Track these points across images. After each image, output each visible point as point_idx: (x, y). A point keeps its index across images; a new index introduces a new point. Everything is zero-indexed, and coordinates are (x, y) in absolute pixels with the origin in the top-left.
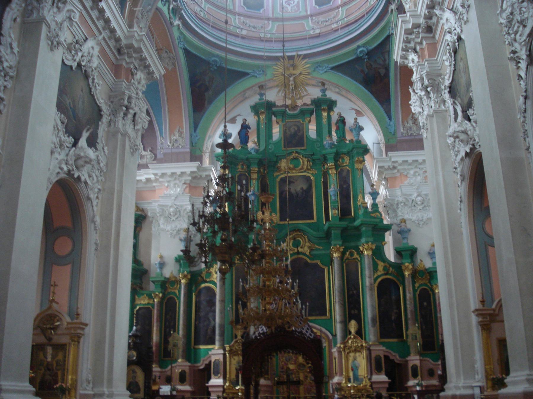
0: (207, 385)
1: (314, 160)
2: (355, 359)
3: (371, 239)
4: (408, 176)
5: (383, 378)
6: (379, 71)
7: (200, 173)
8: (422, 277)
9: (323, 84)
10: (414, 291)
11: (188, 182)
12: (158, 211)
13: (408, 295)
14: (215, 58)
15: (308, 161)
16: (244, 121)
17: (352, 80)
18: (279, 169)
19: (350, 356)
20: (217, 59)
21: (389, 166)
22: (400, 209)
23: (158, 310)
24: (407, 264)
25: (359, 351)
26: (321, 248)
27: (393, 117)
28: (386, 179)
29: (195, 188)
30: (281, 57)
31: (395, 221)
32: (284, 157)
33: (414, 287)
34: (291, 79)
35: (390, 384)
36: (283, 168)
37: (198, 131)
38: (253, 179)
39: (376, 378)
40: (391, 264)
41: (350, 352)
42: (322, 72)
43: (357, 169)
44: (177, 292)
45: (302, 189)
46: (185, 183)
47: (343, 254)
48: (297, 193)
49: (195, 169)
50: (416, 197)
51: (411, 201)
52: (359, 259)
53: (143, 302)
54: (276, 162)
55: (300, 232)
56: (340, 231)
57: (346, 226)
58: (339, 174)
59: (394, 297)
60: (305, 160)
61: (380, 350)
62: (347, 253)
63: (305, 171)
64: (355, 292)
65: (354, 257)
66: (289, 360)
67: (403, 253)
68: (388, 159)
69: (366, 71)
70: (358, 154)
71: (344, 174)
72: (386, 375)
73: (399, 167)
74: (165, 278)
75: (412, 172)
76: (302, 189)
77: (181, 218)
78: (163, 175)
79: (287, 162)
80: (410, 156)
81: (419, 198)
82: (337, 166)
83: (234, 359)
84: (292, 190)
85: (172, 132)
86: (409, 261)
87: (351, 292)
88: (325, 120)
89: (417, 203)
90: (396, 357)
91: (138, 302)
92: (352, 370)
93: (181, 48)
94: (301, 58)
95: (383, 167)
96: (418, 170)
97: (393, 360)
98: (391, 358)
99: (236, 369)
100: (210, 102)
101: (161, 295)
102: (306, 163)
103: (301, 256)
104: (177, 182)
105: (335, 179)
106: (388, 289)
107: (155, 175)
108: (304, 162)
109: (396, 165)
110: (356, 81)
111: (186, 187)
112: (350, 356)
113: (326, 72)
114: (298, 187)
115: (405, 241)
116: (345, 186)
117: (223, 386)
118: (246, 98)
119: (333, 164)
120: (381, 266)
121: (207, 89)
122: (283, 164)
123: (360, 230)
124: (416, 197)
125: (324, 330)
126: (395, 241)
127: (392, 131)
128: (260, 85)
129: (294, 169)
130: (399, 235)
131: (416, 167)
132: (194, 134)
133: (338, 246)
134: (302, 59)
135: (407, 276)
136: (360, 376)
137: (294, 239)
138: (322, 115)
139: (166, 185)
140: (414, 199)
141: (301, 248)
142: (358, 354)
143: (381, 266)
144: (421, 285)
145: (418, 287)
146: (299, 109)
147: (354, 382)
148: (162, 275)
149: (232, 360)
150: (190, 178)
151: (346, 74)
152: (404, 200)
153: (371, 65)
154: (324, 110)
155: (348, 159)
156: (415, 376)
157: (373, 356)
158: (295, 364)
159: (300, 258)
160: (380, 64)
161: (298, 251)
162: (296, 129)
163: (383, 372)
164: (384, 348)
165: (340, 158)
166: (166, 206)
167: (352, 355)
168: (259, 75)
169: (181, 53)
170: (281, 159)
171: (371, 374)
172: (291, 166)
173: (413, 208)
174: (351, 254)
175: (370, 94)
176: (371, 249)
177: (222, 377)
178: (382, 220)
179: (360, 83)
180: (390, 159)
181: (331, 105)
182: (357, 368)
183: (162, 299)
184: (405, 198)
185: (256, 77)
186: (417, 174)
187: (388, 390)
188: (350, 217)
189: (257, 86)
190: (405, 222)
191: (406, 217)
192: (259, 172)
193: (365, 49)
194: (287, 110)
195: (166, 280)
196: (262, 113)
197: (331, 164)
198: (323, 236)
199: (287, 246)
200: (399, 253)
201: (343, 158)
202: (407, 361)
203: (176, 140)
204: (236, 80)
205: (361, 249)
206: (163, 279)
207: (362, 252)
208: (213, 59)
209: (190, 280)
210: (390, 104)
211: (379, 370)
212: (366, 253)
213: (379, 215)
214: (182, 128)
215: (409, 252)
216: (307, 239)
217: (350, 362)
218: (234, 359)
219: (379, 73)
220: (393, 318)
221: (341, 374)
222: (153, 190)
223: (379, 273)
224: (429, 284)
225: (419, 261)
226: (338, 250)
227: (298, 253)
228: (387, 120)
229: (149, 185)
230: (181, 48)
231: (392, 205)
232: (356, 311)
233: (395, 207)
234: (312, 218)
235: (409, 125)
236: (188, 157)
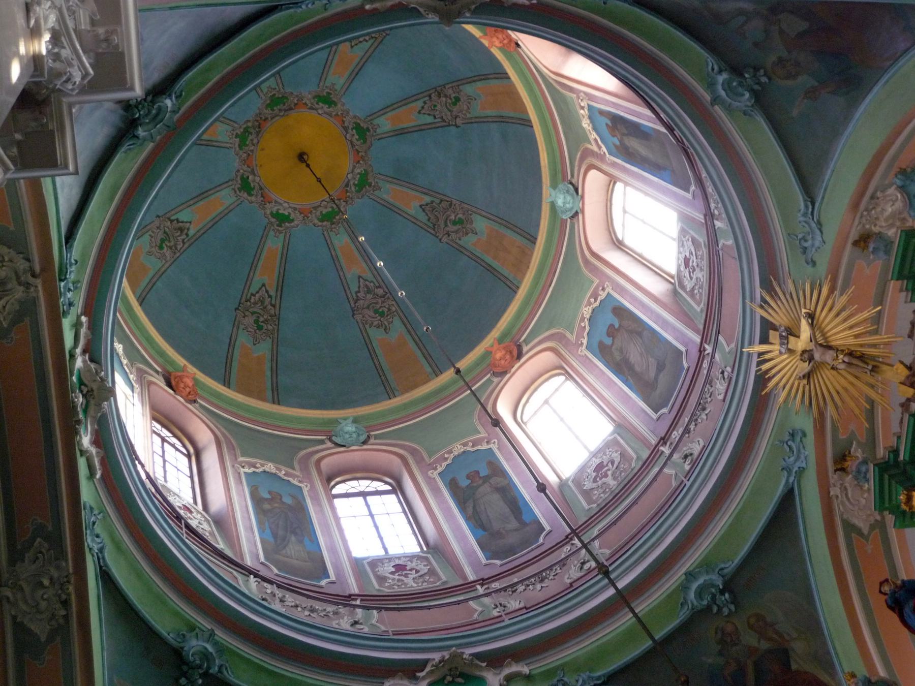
17: (847, 133)
20: (701, 581)
30: (760, 363)
42: (819, 238)
69: (805, 81)
94: (768, 299)
113: (819, 224)
121: (783, 655)
134: (772, 297)
153: (780, 60)
179: (853, 105)
189: (833, 478)
193: (721, 78)
204: (795, 539)
208: (692, 595)
219: (801, 35)
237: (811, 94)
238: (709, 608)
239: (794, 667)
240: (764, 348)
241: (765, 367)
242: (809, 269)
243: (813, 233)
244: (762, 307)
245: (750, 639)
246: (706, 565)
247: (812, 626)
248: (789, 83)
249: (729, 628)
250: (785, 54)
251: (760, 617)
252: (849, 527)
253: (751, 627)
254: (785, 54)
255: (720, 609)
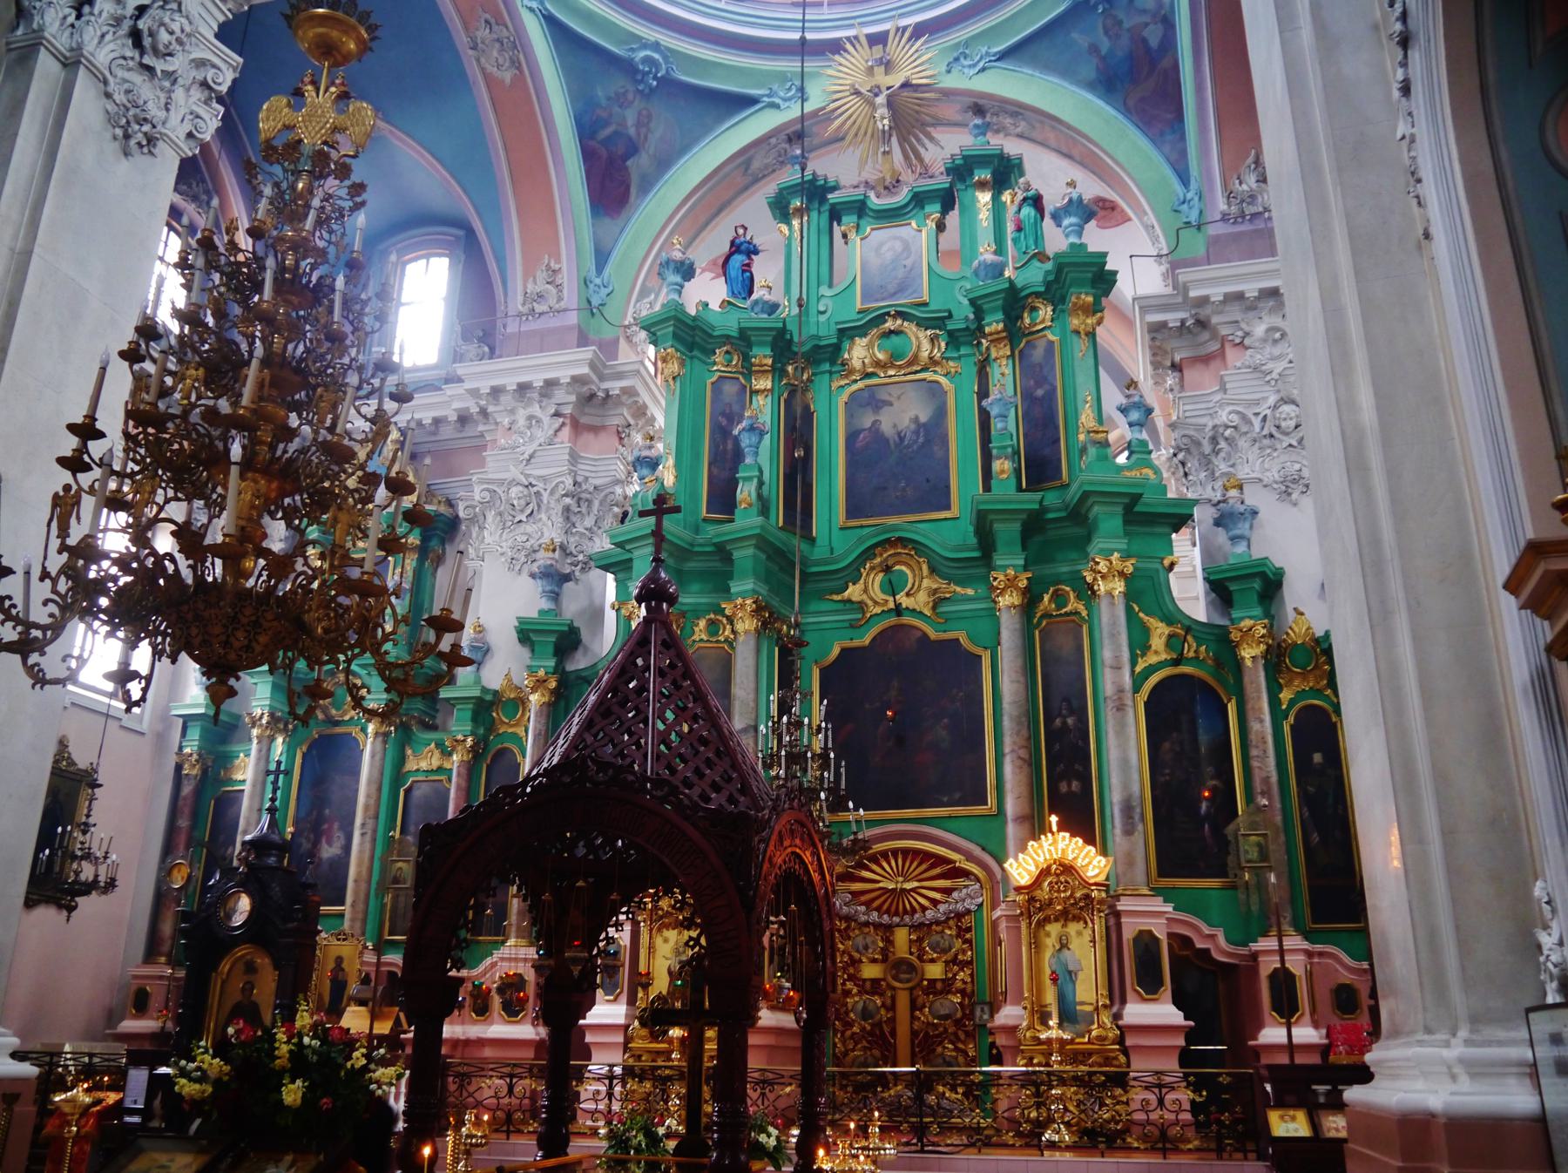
0: (581, 1022)
1: (951, 334)
2: (1064, 945)
3: (1122, 544)
4: (1247, 342)
5: (1165, 1012)
6: (1146, 33)
7: (606, 385)
8: (1303, 668)
9: (979, 110)
10: (1277, 715)
11: (567, 410)
12: (477, 498)
13: (1259, 732)
14: (648, 53)
15: (933, 340)
16: (741, 231)
17: (1066, 84)
18: (846, 370)
19: (1048, 935)
20: (656, 56)
21: (1183, 322)
22: (1222, 454)
23: (458, 787)
24: (1247, 623)
25: (1077, 918)
26: (970, 592)
27: (1194, 171)
28: (1176, 367)
29: (595, 429)
30: (848, 39)
31: (1208, 493)
32: (862, 331)
33: (1274, 702)
34: (881, 100)
35: (1191, 1036)
36: (857, 364)
37: (608, 270)
38: (757, 392)
39: (1137, 1012)
40: (1190, 627)
41: (1047, 920)
42: (972, 72)
43: (1078, 332)
44: (520, 731)
45: (916, 420)
46: (557, 414)
47: (1030, 599)
48: (899, 434)
49: (585, 370)
50: (1275, 407)
51: (1257, 422)
52: (1084, 613)
53: (424, 765)
54: (836, 349)
55: (905, 547)
56: (1017, 526)
57: (1036, 506)
58: (1020, 358)
59: (1204, 738)
60: (924, 336)
61: (1150, 914)
62: (1046, 598)
63: (924, 369)
64: (1070, 721)
65: (1068, 609)
66: (866, 948)
67: (1233, 587)
68: (1180, 300)
69: (1105, 45)
70: (1079, 283)
71: (1038, 354)
72: (1175, 1003)
73: (1215, 320)
74: (484, 690)
75: (1259, 330)
76: (916, 420)
77: (543, 516)
78: (496, 392)
79: (870, 346)
80: (1249, 276)
81: (1287, 408)
82: (1014, 333)
83: (666, 940)
84: (887, 428)
85: (529, 273)
86: (1258, 611)
87: (1058, 722)
88: (984, 216)
89: (1278, 427)
90: (1218, 943)
91: (411, 765)
92: (1055, 980)
93: (531, 10)
94: (907, 35)
95: (1164, 325)
96: (1276, 321)
97: (1208, 951)
98: (1199, 945)
99: (670, 972)
100: (647, 185)
101: (469, 740)
102: (926, 346)
103: (907, 619)
104: (535, 410)
105: (1008, 371)
106: (1185, 713)
107: (474, 393)
108: (921, 341)
109: (1204, 312)
110: (1079, 83)
111: (563, 424)
112: (1048, 935)
113: (983, 69)
114: (903, 413)
115: (1241, 548)
116: (1040, 392)
117: (626, 1027)
118: (756, 180)
119: (1001, 326)
120: (1159, 632)
121: (633, 149)
122: (859, 353)
123: (1087, 518)
124: (1275, 407)
125: (977, 851)
126: (1207, 554)
127: (1193, 217)
128: (789, 131)
129: (893, 366)
130: (1221, 536)
131: (1271, 311)
132: (598, 281)
133: (1011, 572)
135: (1249, 663)
136: (1082, 1003)
137: (887, 569)
138: (975, 200)
139: (506, 421)
140: (1268, 412)
141: (908, 595)
142: (1073, 928)
143: (1159, 632)
144: (1300, 695)
145: (1292, 702)
146: (905, 190)
147: (1060, 1026)
148: (478, 681)
149: (659, 941)
150: (573, 398)
151: (1048, 67)
152: (1234, 417)
153: (1120, 23)
154: (982, 185)
155: (1049, 309)
156: (1287, 1009)
157: (1128, 934)
158: (884, 960)
159: (903, 626)
160: (1144, 11)
161: (898, 606)
162: (898, 246)
163: (1167, 991)
164: (1169, 908)
165: (1024, 308)
166: (501, 482)
167: (1054, 929)
168: (790, 99)
169: (535, 30)
170: (852, 338)
171: (1123, 1002)
172: (881, 356)
173: (1267, 442)
174: (1059, 598)
175: (1120, 117)
176: (1121, 574)
177: (624, 998)
178: (1164, 489)
179: (1091, 86)
180: (1186, 289)
181: (1004, 172)
182: (1071, 975)
183: (477, 753)
184: (1238, 413)
185: (777, 107)
186: (1277, 335)
187: (1186, 1057)
188: (1058, 483)
189: (783, 136)
190: (1241, 487)
191: (1243, 472)
192: (778, 371)
194: (872, 194)
195: (489, 697)
196: (799, 212)
197: (994, 324)
198: (976, 554)
199: (866, 591)
200: (1221, 589)
201: (1034, 309)
202: (1254, 956)
203: (540, 296)
204: (720, 120)
205: (1089, 579)
206: (477, 693)
207: (1091, 587)
208: (643, 54)
209: (556, 693)
210: (1183, 138)
211: (1150, 985)
212: (1102, 587)
213: (1152, 476)
214: (558, 261)
215: (1257, 585)
216: (925, 567)
217: (1048, 954)
218: (666, 940)
219: (1144, 41)
220: (1204, 806)
221: (1018, 1000)
222: (479, 448)
223: (1153, 659)
224: (1329, 692)
225: (1291, 615)
226: (1011, 583)
227: (898, 610)
228: (1178, 187)
229: (470, 431)
230: (531, 10)
231: (1199, 444)
232: (1075, 785)
233: (1207, 448)
234: (948, 507)
235: (1245, 187)
236: (574, 336)
237: (1094, 49)
238: (637, 71)
239: (629, 163)
240: (864, 40)
241: (848, 46)
242: (944, 68)
243: (974, 66)
244: (898, 29)
245: (630, 117)
246: (669, 53)
247: (664, 163)
248: (1101, 30)
249: (630, 96)
250: (1126, 25)
251: (649, 117)
252: (748, 163)
253: (640, 113)
254: (1126, 25)
255: (642, 81)
